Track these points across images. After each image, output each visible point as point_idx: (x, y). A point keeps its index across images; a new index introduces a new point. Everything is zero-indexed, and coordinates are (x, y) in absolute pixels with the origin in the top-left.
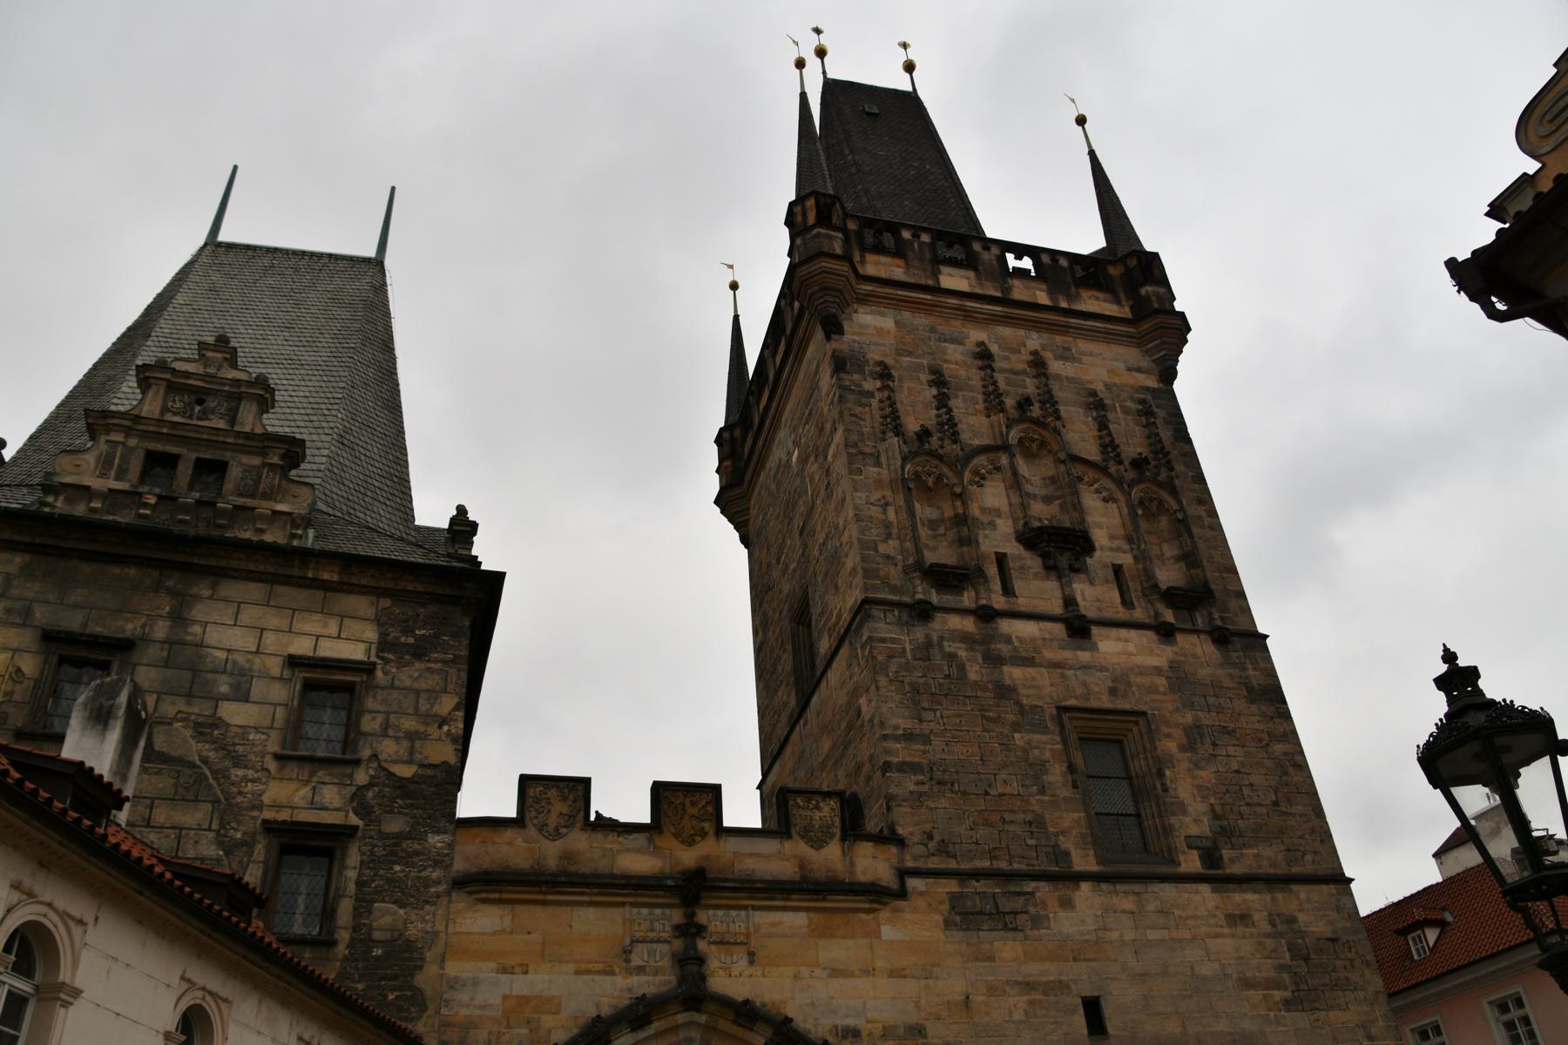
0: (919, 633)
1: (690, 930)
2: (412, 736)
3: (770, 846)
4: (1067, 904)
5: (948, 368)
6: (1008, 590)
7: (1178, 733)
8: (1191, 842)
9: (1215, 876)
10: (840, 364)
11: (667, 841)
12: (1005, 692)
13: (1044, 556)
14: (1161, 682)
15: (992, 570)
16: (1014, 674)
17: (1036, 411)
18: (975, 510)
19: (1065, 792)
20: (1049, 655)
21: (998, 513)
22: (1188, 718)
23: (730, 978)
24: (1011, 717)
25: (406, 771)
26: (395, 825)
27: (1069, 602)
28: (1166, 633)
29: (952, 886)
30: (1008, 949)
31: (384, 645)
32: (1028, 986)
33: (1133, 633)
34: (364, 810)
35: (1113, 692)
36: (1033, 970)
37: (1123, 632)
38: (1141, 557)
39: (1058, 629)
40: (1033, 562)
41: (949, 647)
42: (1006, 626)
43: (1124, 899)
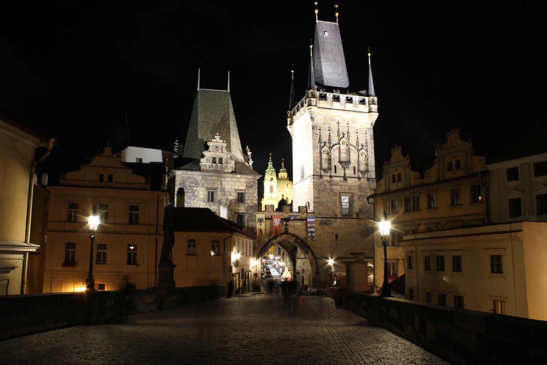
0: (321, 180)
1: (286, 225)
2: (252, 200)
3: (298, 214)
4: (336, 222)
5: (332, 127)
6: (335, 172)
7: (357, 196)
8: (355, 213)
9: (358, 218)
10: (313, 128)
11: (284, 213)
12: (332, 190)
13: (343, 166)
14: (357, 188)
15: (333, 168)
16: (334, 187)
17: (346, 136)
18: (332, 157)
19: (339, 206)
20: (340, 184)
21: (336, 157)
22: (359, 194)
23: (291, 231)
24: (332, 194)
25: (251, 205)
26: (251, 212)
27: (345, 174)
28: (359, 178)
29: (320, 219)
30: (327, 228)
31: (247, 186)
32: (329, 233)
33: (354, 179)
34: (247, 210)
35: (349, 190)
36: (330, 231)
37: (353, 179)
38: (359, 165)
39: (342, 179)
40: (340, 166)
41: (325, 183)
42: (334, 178)
43: (344, 221)
